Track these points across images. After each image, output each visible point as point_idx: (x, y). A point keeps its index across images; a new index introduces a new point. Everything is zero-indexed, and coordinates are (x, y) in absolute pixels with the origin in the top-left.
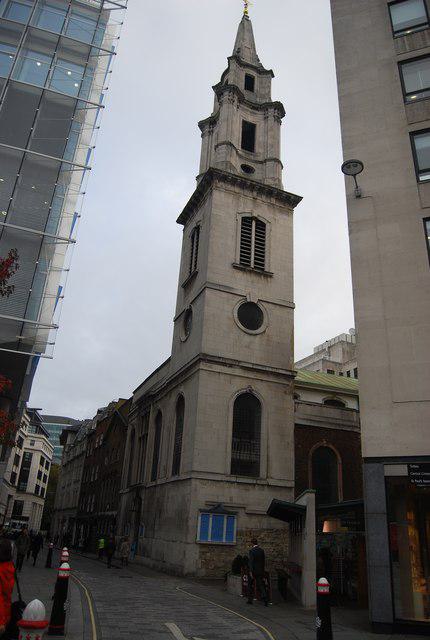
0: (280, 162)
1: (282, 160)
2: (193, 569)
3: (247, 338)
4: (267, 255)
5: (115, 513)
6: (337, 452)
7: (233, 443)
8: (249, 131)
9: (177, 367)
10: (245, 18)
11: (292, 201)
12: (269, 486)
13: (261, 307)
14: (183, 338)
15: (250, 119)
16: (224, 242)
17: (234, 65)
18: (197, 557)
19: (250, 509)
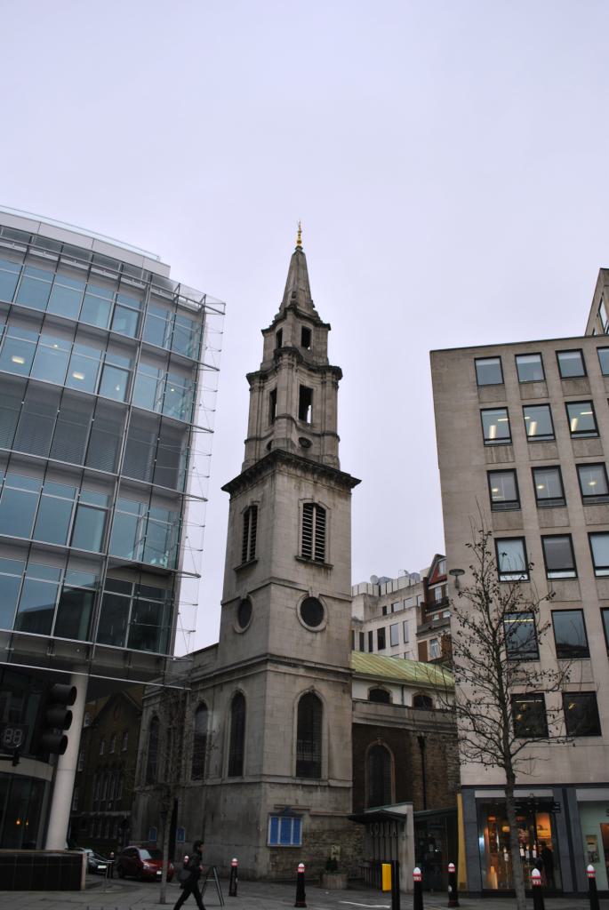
0: (337, 438)
1: (339, 434)
2: (265, 872)
3: (309, 636)
4: (327, 544)
5: (125, 814)
6: (389, 749)
7: (298, 744)
8: (306, 396)
9: (230, 659)
11: (348, 482)
12: (329, 786)
13: (323, 603)
14: (239, 629)
15: (307, 383)
16: (285, 533)
18: (268, 859)
19: (314, 810)
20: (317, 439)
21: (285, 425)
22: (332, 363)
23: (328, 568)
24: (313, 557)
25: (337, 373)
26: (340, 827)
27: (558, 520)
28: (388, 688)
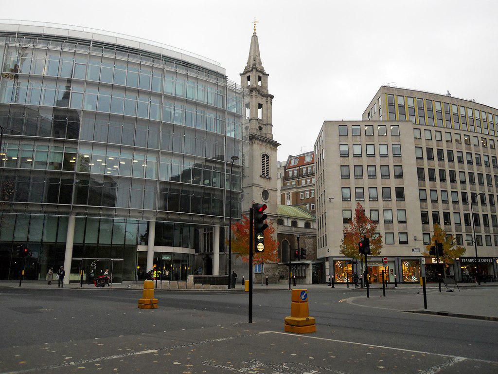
10: (255, 37)
11: (275, 145)
15: (261, 103)
17: (254, 70)
20: (264, 126)
21: (255, 122)
22: (270, 93)
23: (270, 179)
24: (266, 175)
25: (272, 97)
26: (274, 267)
27: (360, 183)
28: (284, 219)
